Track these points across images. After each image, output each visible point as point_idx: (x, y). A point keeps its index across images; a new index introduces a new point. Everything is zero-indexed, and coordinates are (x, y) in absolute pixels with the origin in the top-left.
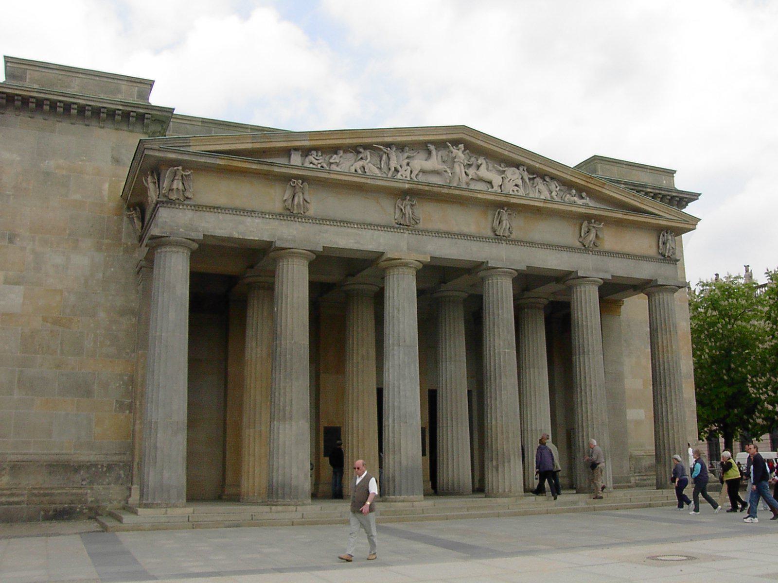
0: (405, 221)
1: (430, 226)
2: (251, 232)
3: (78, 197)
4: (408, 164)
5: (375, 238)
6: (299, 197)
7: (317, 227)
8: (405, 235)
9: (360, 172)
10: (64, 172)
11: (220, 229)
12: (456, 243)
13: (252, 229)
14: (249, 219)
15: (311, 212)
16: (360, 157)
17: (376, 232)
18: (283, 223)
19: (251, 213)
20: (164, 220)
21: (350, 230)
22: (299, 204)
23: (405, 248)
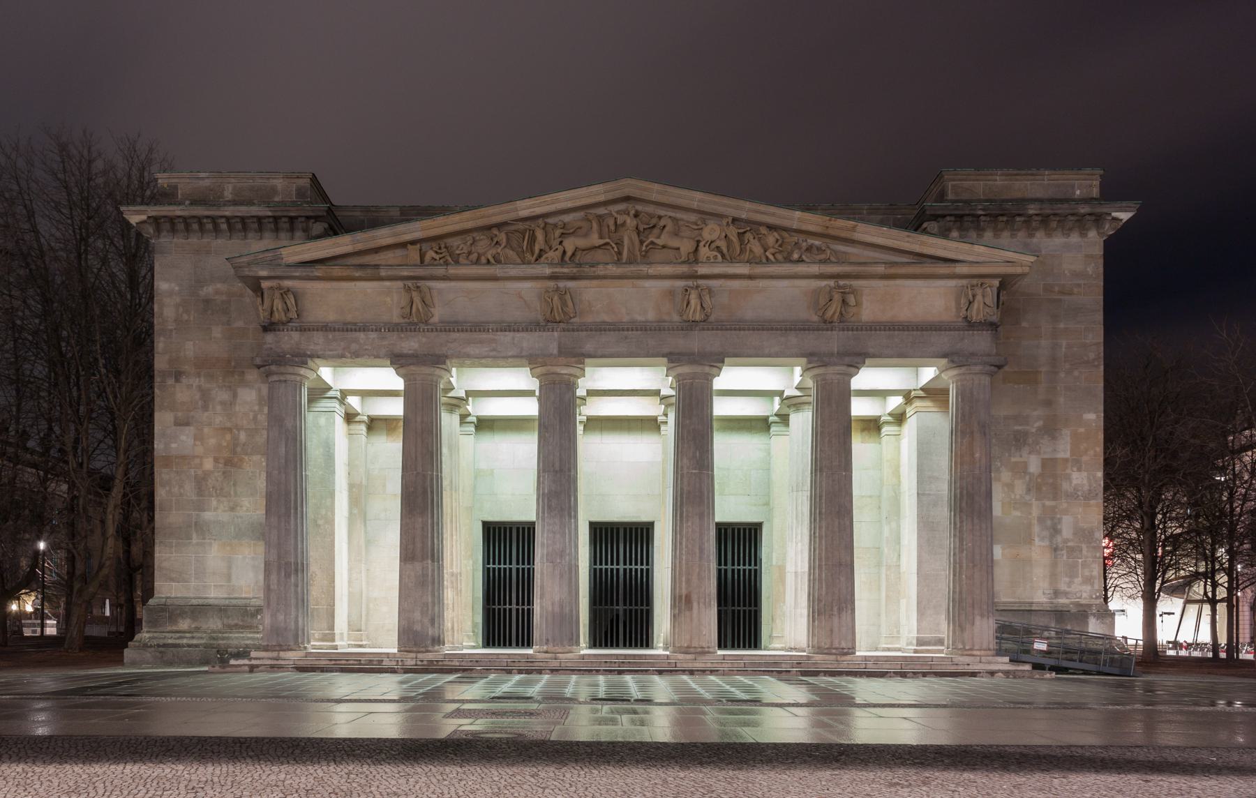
0: (555, 319)
1: (589, 319)
2: (366, 349)
3: (239, 324)
4: (561, 243)
5: (516, 342)
6: (417, 305)
7: (443, 336)
8: (556, 334)
9: (492, 260)
10: (224, 298)
11: (331, 350)
12: (626, 338)
13: (367, 347)
14: (362, 335)
15: (435, 319)
16: (495, 242)
17: (518, 335)
18: (403, 335)
19: (364, 328)
20: (269, 346)
21: (484, 336)
22: (418, 309)
23: (556, 352)
